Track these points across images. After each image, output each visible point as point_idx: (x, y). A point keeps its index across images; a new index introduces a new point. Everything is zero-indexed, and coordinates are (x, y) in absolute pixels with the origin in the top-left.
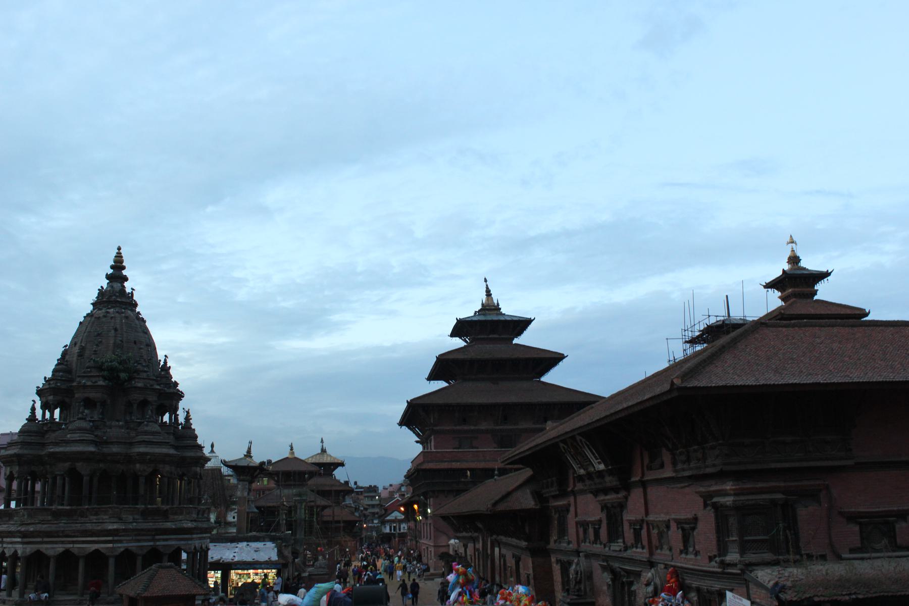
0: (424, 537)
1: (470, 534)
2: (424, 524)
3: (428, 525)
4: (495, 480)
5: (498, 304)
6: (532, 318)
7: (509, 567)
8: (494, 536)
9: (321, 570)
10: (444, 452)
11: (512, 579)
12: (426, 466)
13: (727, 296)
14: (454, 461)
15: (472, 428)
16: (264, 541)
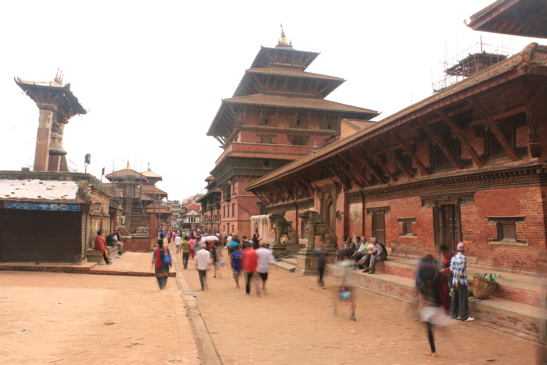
0: (224, 217)
1: (291, 201)
2: (224, 207)
3: (231, 206)
4: (314, 153)
5: (291, 43)
6: (318, 53)
7: (399, 220)
8: (355, 189)
9: (143, 234)
10: (250, 144)
11: (410, 236)
12: (235, 155)
13: (481, 36)
14: (258, 152)
15: (273, 128)
16: (64, 180)
